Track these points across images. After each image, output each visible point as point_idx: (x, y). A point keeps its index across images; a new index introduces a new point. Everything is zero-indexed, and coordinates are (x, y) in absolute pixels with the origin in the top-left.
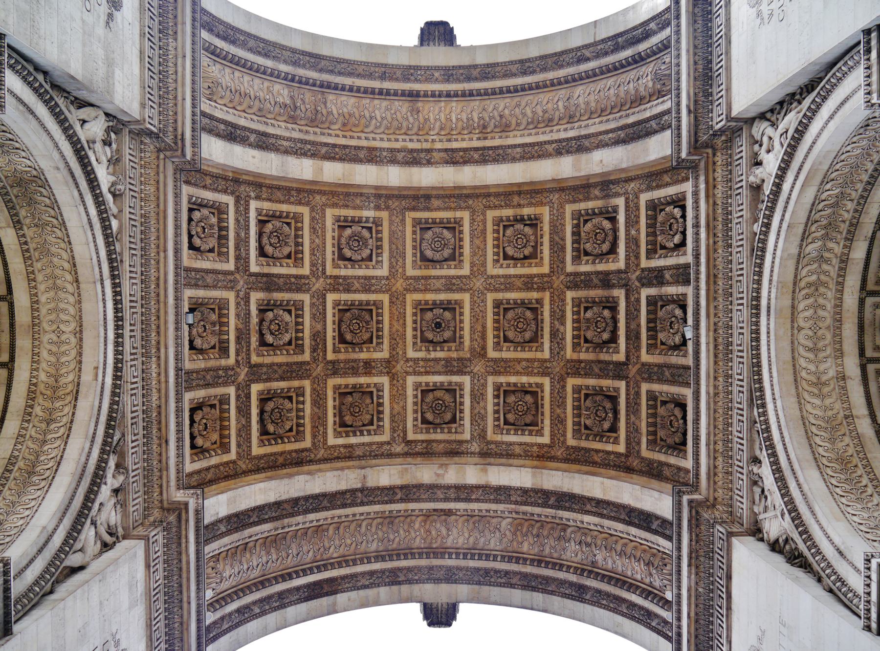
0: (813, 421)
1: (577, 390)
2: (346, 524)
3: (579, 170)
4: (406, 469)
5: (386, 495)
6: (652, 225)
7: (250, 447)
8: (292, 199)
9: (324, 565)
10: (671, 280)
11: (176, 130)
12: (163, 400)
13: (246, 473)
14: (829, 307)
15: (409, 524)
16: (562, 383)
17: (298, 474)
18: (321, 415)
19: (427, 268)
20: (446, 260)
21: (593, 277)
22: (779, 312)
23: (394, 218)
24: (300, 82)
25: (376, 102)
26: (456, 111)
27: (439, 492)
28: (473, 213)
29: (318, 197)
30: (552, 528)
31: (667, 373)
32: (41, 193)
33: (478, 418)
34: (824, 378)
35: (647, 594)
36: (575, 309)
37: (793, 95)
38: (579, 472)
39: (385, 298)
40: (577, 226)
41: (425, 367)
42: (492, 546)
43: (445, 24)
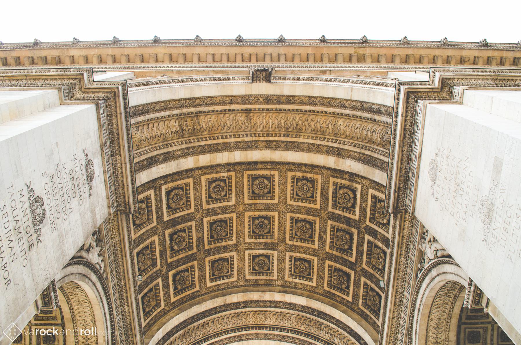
3: (338, 166)
4: (245, 295)
12: (132, 319)
13: (169, 311)
15: (247, 316)
16: (323, 261)
22: (423, 315)
23: (238, 175)
29: (197, 172)
30: (315, 323)
39: (234, 215)
40: (336, 189)
41: (255, 246)
42: (286, 325)
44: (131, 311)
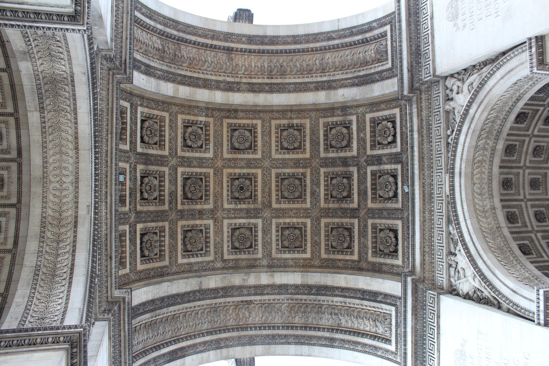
0: (484, 230)
1: (327, 225)
2: (189, 313)
3: (330, 99)
4: (225, 277)
5: (214, 294)
6: (373, 132)
7: (136, 264)
8: (159, 108)
9: (178, 339)
10: (386, 161)
11: (121, 57)
14: (486, 172)
15: (226, 311)
16: (318, 222)
17: (165, 281)
18: (174, 244)
19: (235, 153)
20: (246, 149)
21: (337, 160)
24: (167, 36)
25: (208, 52)
26: (254, 61)
27: (245, 290)
28: (263, 121)
29: (174, 107)
30: (313, 307)
31: (385, 213)
32: (65, 89)
33: (267, 244)
34: (486, 209)
35: (374, 337)
36: (326, 179)
37: (474, 66)
38: (329, 272)
40: (326, 131)
41: (235, 214)
42: (276, 321)
43: (249, 11)
44: (109, 217)
